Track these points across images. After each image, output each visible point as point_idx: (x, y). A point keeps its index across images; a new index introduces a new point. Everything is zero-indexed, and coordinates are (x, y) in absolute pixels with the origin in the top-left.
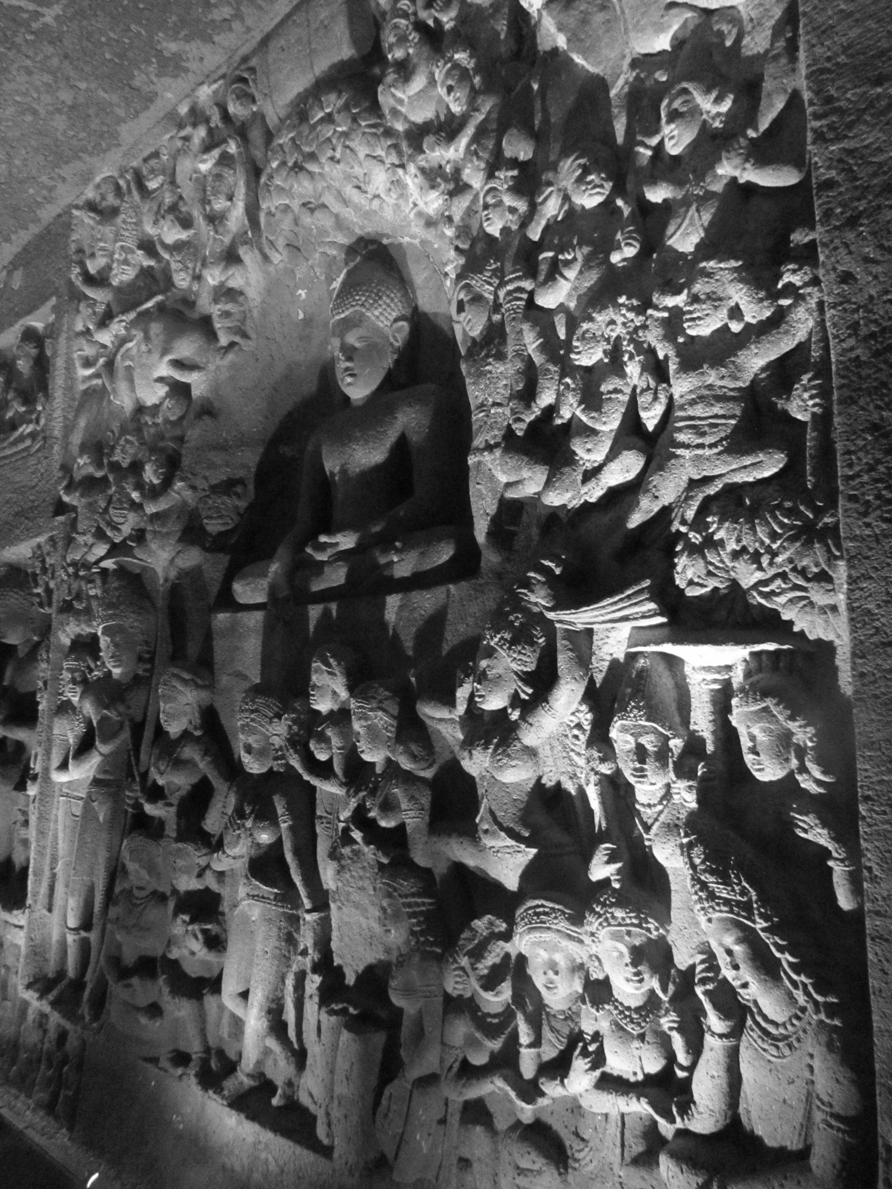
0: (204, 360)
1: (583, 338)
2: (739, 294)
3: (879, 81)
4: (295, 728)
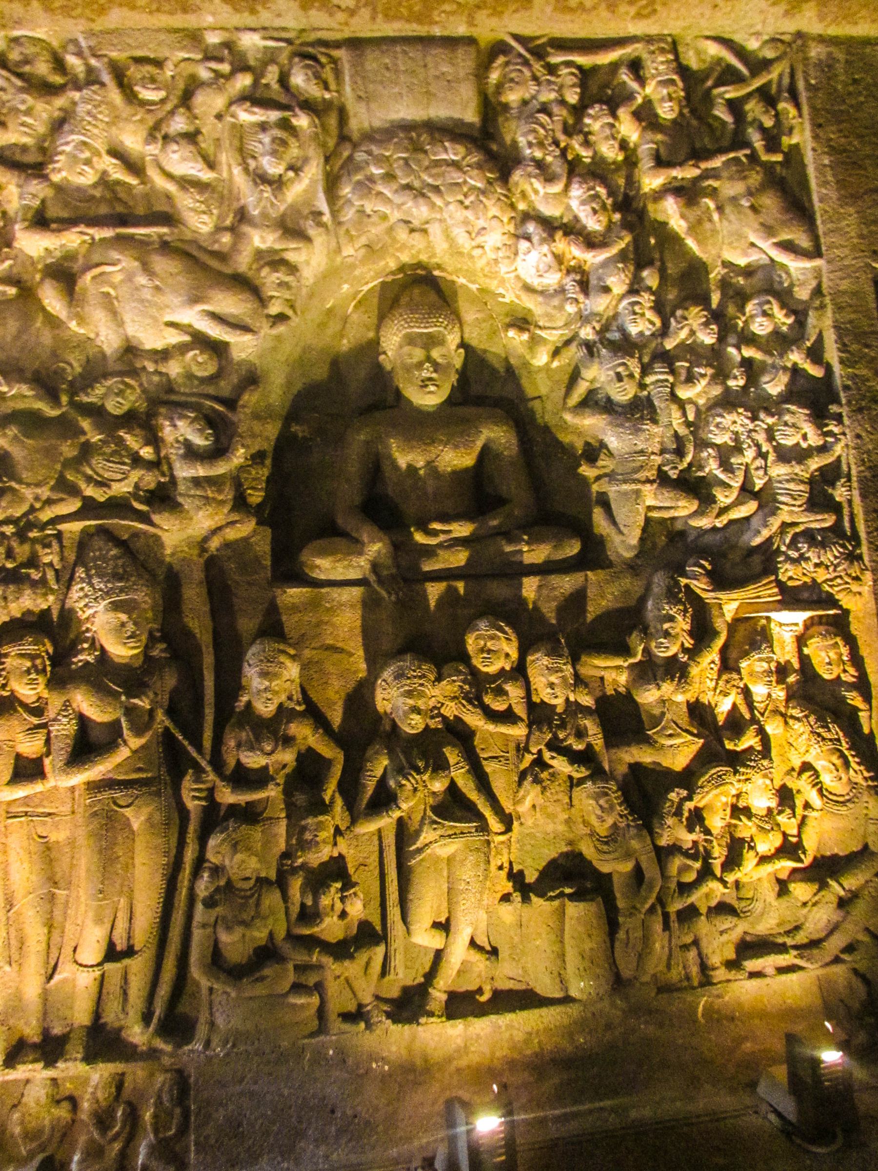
0: (258, 325)
1: (717, 426)
2: (808, 428)
3: (867, 346)
4: (467, 687)
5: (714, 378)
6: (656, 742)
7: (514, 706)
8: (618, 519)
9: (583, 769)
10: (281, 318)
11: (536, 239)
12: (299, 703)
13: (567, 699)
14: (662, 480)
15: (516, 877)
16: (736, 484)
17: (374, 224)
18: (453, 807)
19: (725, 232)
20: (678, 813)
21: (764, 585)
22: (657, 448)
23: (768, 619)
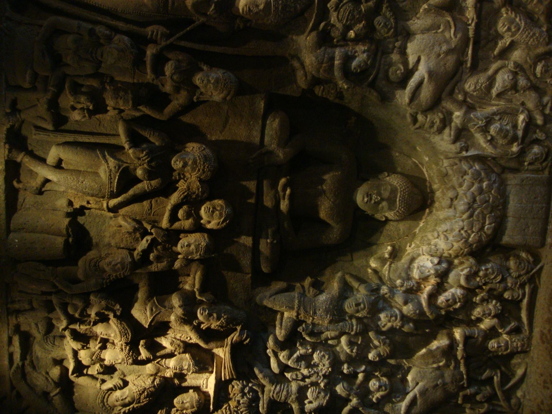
0: (413, 107)
1: (324, 356)
2: (315, 405)
4: (194, 196)
5: (349, 356)
6: (149, 301)
7: (180, 222)
8: (279, 296)
9: (139, 257)
10: (415, 120)
11: (438, 267)
12: (198, 98)
13: (180, 254)
14: (297, 323)
15: (82, 211)
16: (290, 363)
17: (458, 179)
18: (127, 179)
19: (426, 370)
20: (108, 309)
21: (231, 372)
22: (316, 321)
23: (212, 372)
